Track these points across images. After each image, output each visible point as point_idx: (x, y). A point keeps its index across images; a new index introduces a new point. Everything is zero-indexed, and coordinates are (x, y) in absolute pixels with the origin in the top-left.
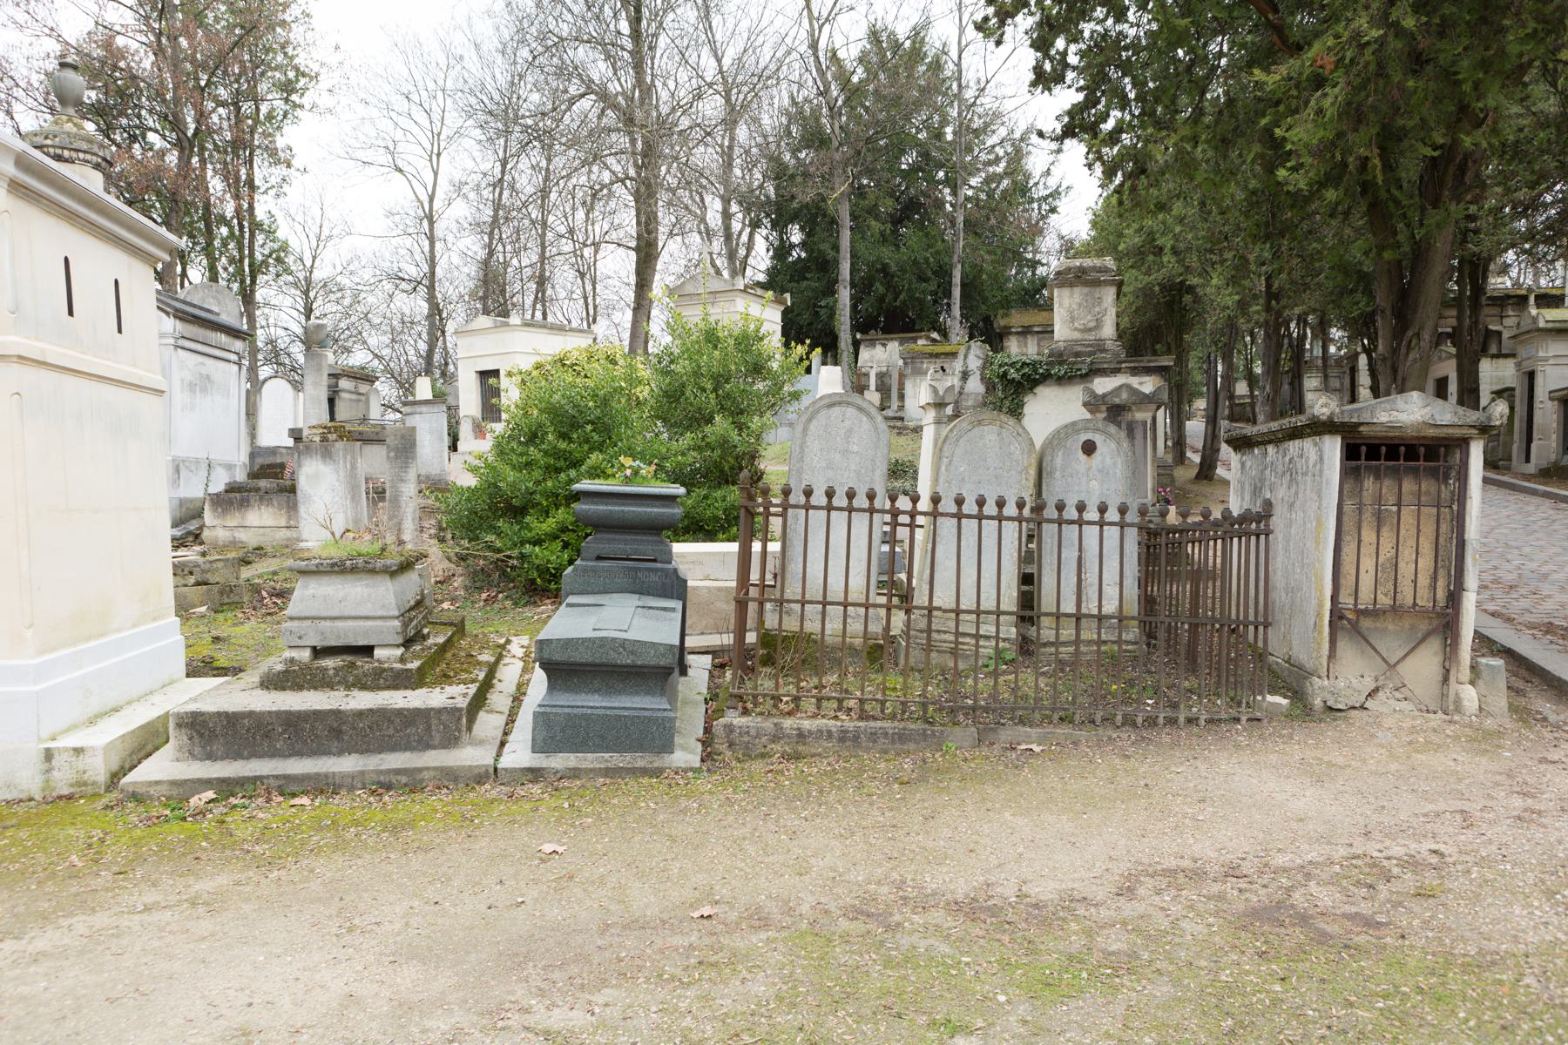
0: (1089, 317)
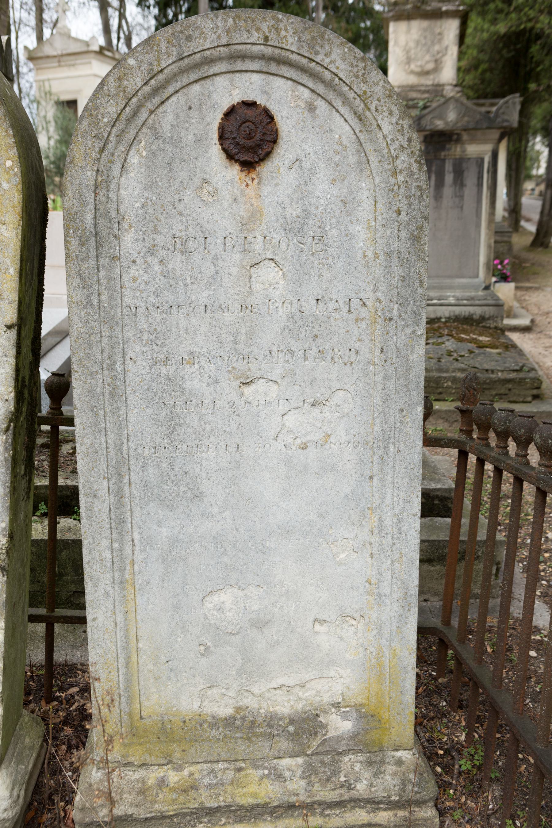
0: (428, 58)
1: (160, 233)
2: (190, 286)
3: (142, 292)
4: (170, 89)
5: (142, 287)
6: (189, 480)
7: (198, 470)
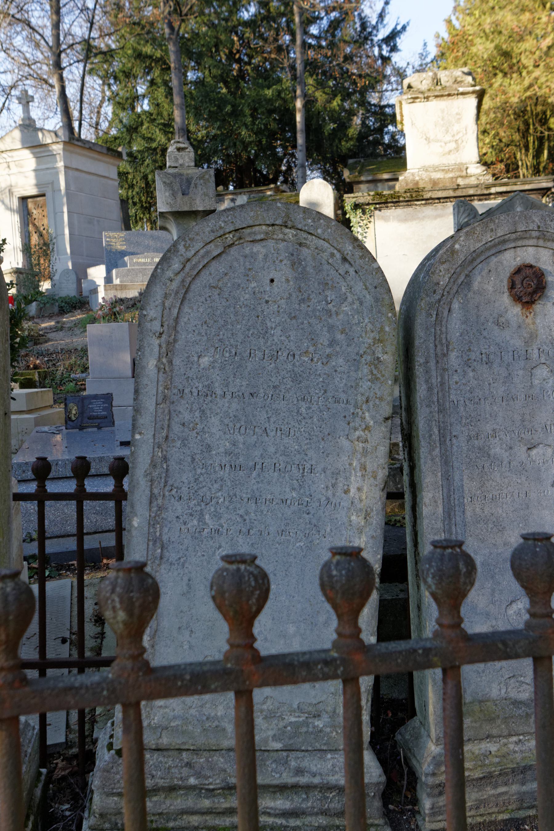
1: (473, 351)
2: (492, 385)
3: (461, 391)
4: (478, 261)
5: (461, 388)
6: (495, 520)
7: (500, 511)
